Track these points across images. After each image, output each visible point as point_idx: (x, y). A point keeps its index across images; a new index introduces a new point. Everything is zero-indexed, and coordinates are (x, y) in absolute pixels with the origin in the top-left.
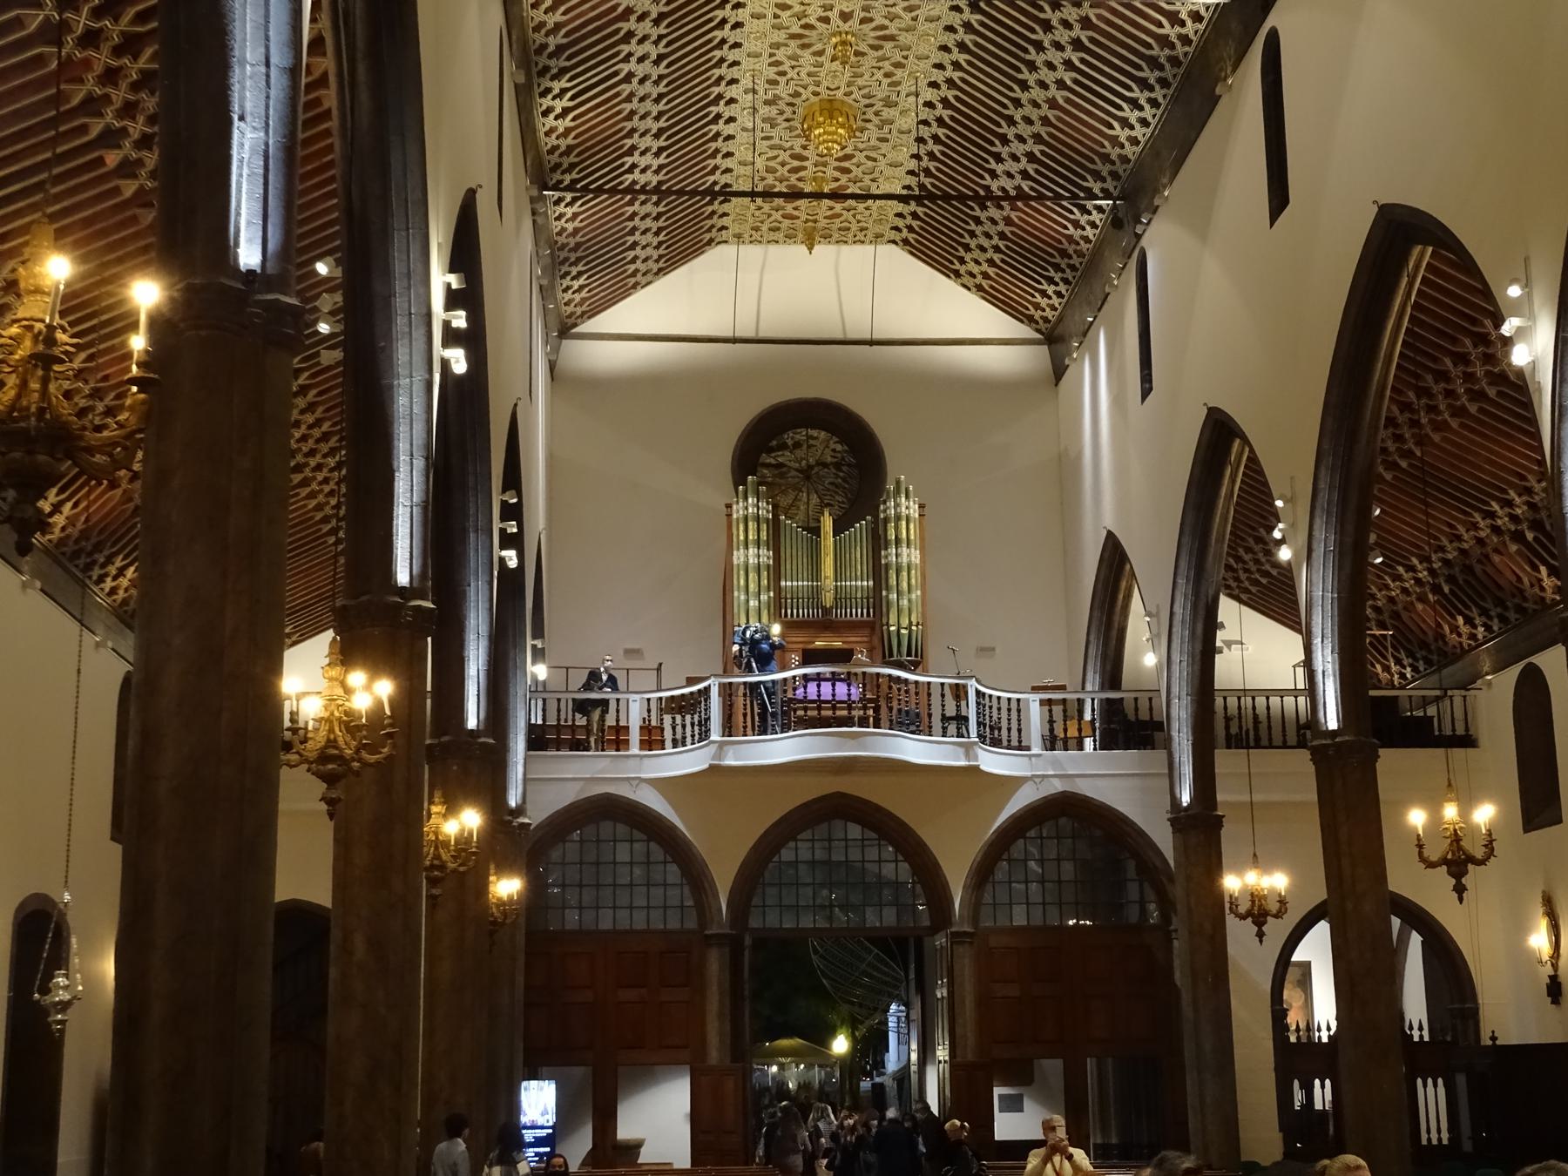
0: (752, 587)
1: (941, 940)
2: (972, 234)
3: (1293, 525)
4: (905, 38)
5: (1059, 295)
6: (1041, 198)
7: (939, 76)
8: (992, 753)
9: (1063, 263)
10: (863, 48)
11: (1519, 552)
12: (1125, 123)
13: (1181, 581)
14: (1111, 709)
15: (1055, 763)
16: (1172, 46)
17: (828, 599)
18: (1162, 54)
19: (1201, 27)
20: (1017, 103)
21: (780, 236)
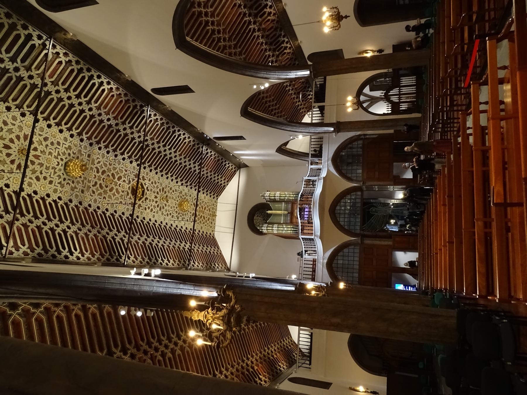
0: (282, 229)
2: (214, 181)
4: (163, 186)
5: (229, 164)
10: (165, 195)
12: (185, 138)
13: (283, 128)
15: (325, 162)
16: (163, 123)
17: (286, 212)
18: (165, 126)
19: (158, 114)
20: (181, 164)
21: (213, 222)
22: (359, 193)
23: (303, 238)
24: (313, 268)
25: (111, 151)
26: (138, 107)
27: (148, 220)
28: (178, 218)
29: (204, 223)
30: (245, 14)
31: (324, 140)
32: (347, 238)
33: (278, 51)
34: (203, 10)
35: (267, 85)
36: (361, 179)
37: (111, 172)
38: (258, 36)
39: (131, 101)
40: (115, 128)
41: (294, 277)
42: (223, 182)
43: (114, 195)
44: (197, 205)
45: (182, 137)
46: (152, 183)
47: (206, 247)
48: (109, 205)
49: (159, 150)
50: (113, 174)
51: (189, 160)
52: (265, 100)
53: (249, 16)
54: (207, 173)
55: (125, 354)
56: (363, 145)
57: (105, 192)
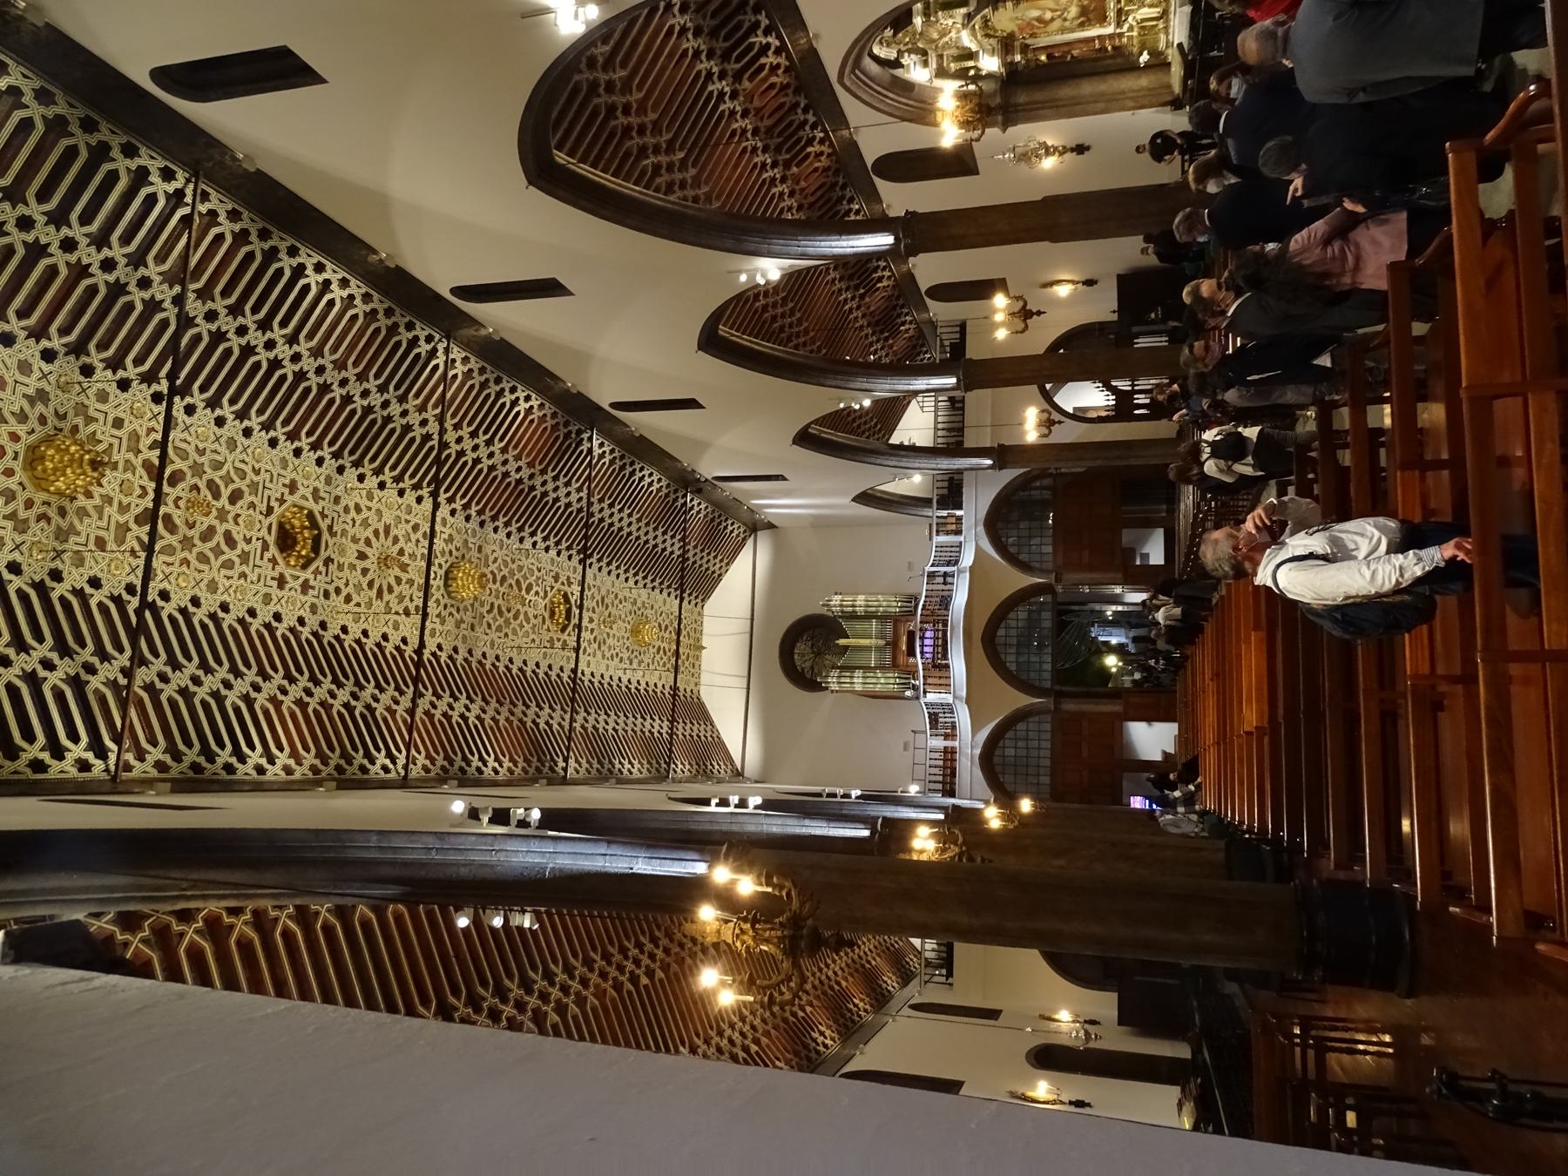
1: (1059, 589)
3: (853, 399)
4: (603, 592)
6: (684, 529)
7: (623, 577)
8: (964, 562)
12: (650, 484)
14: (944, 503)
15: (969, 529)
17: (881, 642)
20: (638, 538)
32: (1024, 700)
36: (1050, 566)
43: (522, 626)
44: (679, 633)
45: (647, 480)
50: (518, 582)
57: (507, 622)
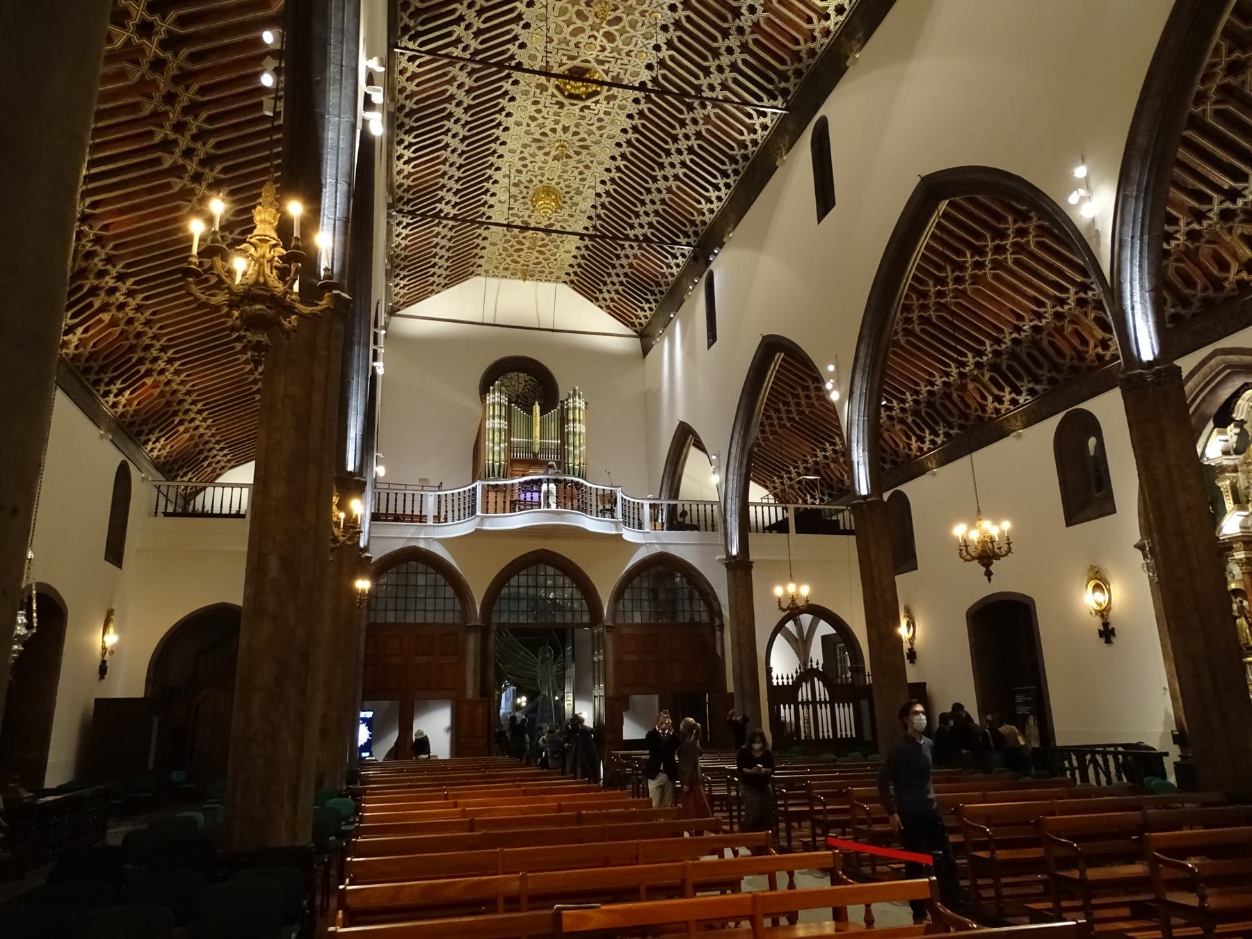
0: (496, 439)
2: (609, 275)
4: (594, 148)
5: (651, 309)
9: (656, 290)
10: (571, 153)
11: (901, 430)
12: (709, 201)
13: (736, 436)
15: (657, 537)
16: (746, 147)
17: (537, 449)
18: (738, 153)
19: (766, 133)
20: (649, 191)
21: (508, 273)
22: (586, 619)
23: (474, 489)
24: (404, 515)
25: (676, 16)
26: (782, 85)
27: (508, 110)
28: (515, 185)
29: (505, 249)
30: (998, 341)
31: (710, 533)
32: (478, 594)
33: (914, 421)
34: (1011, 240)
35: (835, 396)
37: (624, 16)
38: (948, 374)
39: (796, 65)
40: (732, 25)
41: (380, 471)
42: (607, 296)
44: (547, 231)
45: (713, 194)
46: (600, 120)
47: (447, 255)
48: (543, 10)
49: (680, 136)
50: (618, 20)
51: (656, 213)
52: (802, 395)
53: (995, 353)
54: (627, 257)
55: (163, 45)
56: (699, 624)
